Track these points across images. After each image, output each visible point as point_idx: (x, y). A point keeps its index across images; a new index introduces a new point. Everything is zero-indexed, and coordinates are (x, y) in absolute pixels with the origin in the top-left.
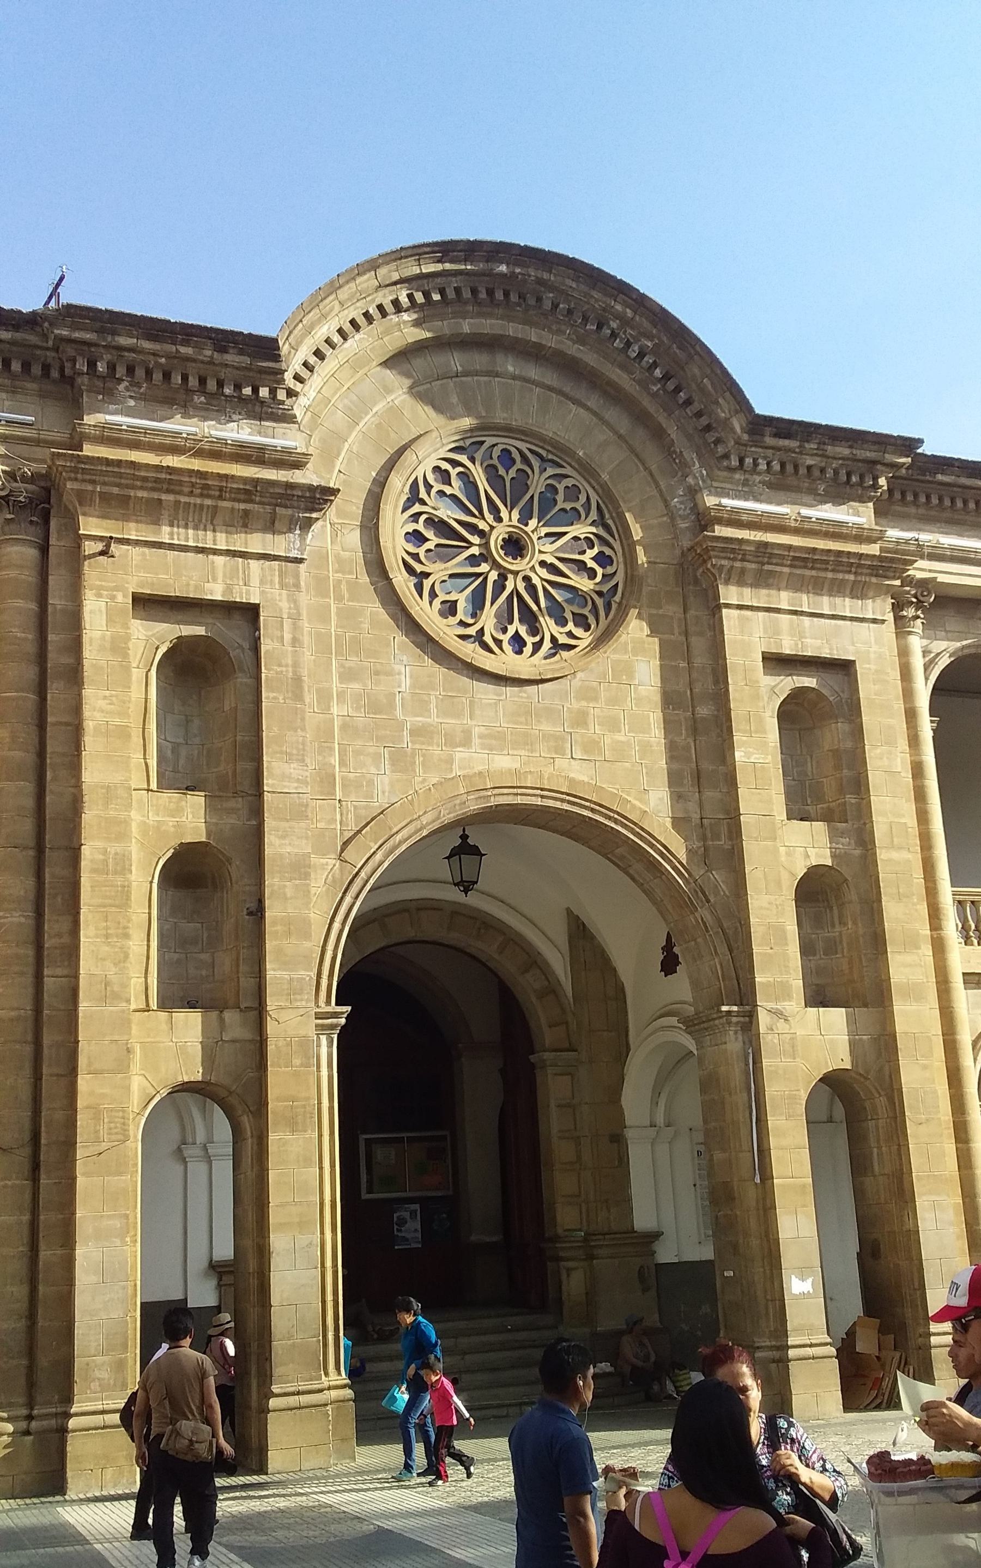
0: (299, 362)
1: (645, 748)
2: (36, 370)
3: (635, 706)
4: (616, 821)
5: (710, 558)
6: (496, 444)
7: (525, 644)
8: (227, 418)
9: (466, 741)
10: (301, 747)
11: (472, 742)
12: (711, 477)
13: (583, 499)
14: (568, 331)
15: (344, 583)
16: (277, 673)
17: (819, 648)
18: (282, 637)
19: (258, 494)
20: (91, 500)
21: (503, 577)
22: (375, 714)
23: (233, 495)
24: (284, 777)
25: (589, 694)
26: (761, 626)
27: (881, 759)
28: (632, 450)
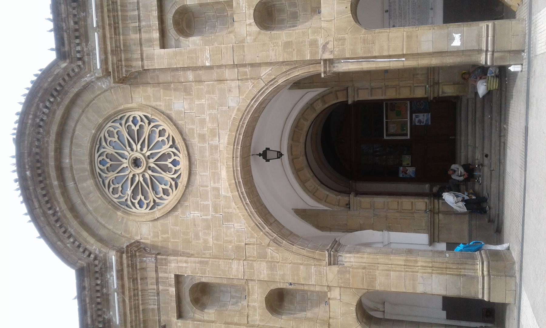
0: (83, 255)
3: (193, 110)
4: (244, 123)
5: (123, 77)
6: (98, 167)
7: (174, 160)
9: (217, 189)
10: (226, 263)
11: (217, 187)
12: (90, 71)
14: (46, 139)
15: (162, 236)
16: (199, 270)
18: (186, 267)
19: (133, 276)
21: (150, 168)
22: (211, 227)
23: (136, 285)
24: (238, 271)
26: (148, 49)
28: (88, 105)
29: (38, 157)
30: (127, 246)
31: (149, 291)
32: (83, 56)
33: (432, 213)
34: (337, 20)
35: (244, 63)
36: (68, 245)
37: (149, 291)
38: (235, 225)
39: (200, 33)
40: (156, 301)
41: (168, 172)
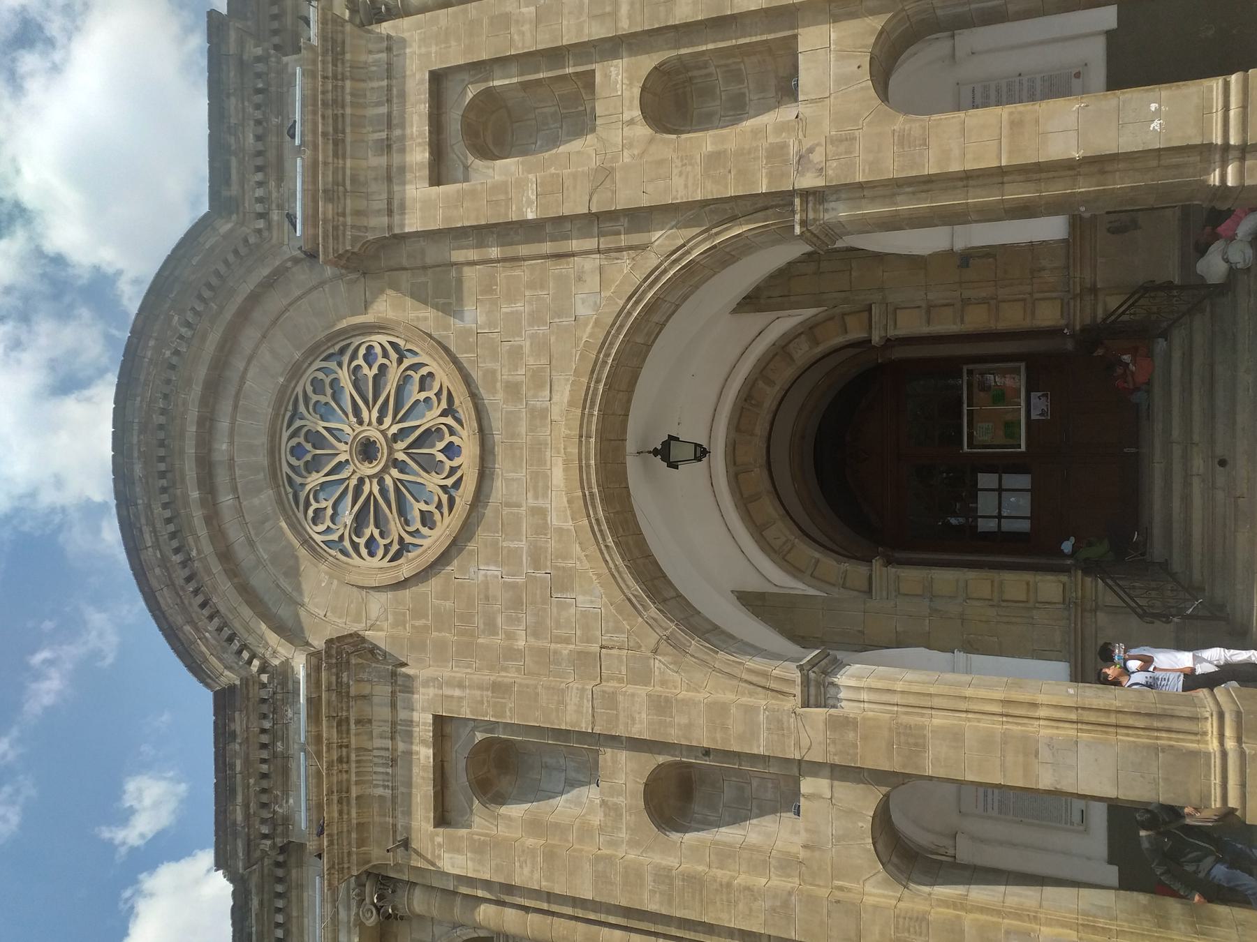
1: (536, 319)
4: (607, 355)
5: (347, 251)
7: (451, 443)
8: (292, 721)
9: (540, 512)
13: (321, 375)
14: (183, 396)
16: (488, 706)
18: (461, 698)
19: (340, 714)
20: (365, 853)
21: (396, 463)
24: (579, 711)
27: (523, 34)
28: (274, 322)
29: (162, 435)
30: (330, 642)
31: (376, 753)
32: (269, 209)
33: (1080, 608)
34: (835, 98)
35: (613, 209)
36: (207, 634)
37: (376, 753)
38: (580, 598)
39: (524, 153)
40: (390, 778)
41: (434, 473)
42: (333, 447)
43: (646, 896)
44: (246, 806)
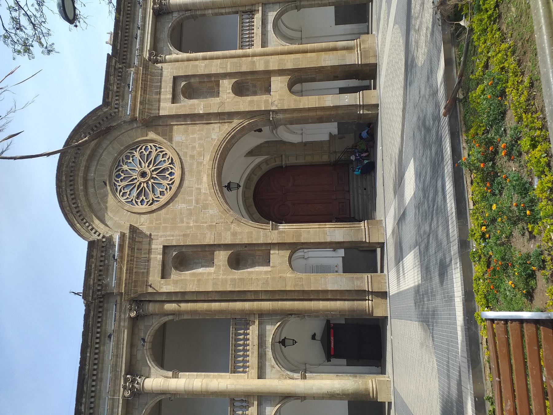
1: (200, 139)
2: (101, 304)
4: (221, 148)
13: (129, 154)
16: (182, 241)
17: (170, 86)
18: (173, 240)
21: (153, 178)
24: (210, 239)
25: (186, 154)
28: (114, 139)
29: (72, 169)
31: (142, 259)
37: (142, 259)
38: (210, 211)
40: (147, 266)
42: (131, 174)
43: (228, 286)
44: (94, 280)
